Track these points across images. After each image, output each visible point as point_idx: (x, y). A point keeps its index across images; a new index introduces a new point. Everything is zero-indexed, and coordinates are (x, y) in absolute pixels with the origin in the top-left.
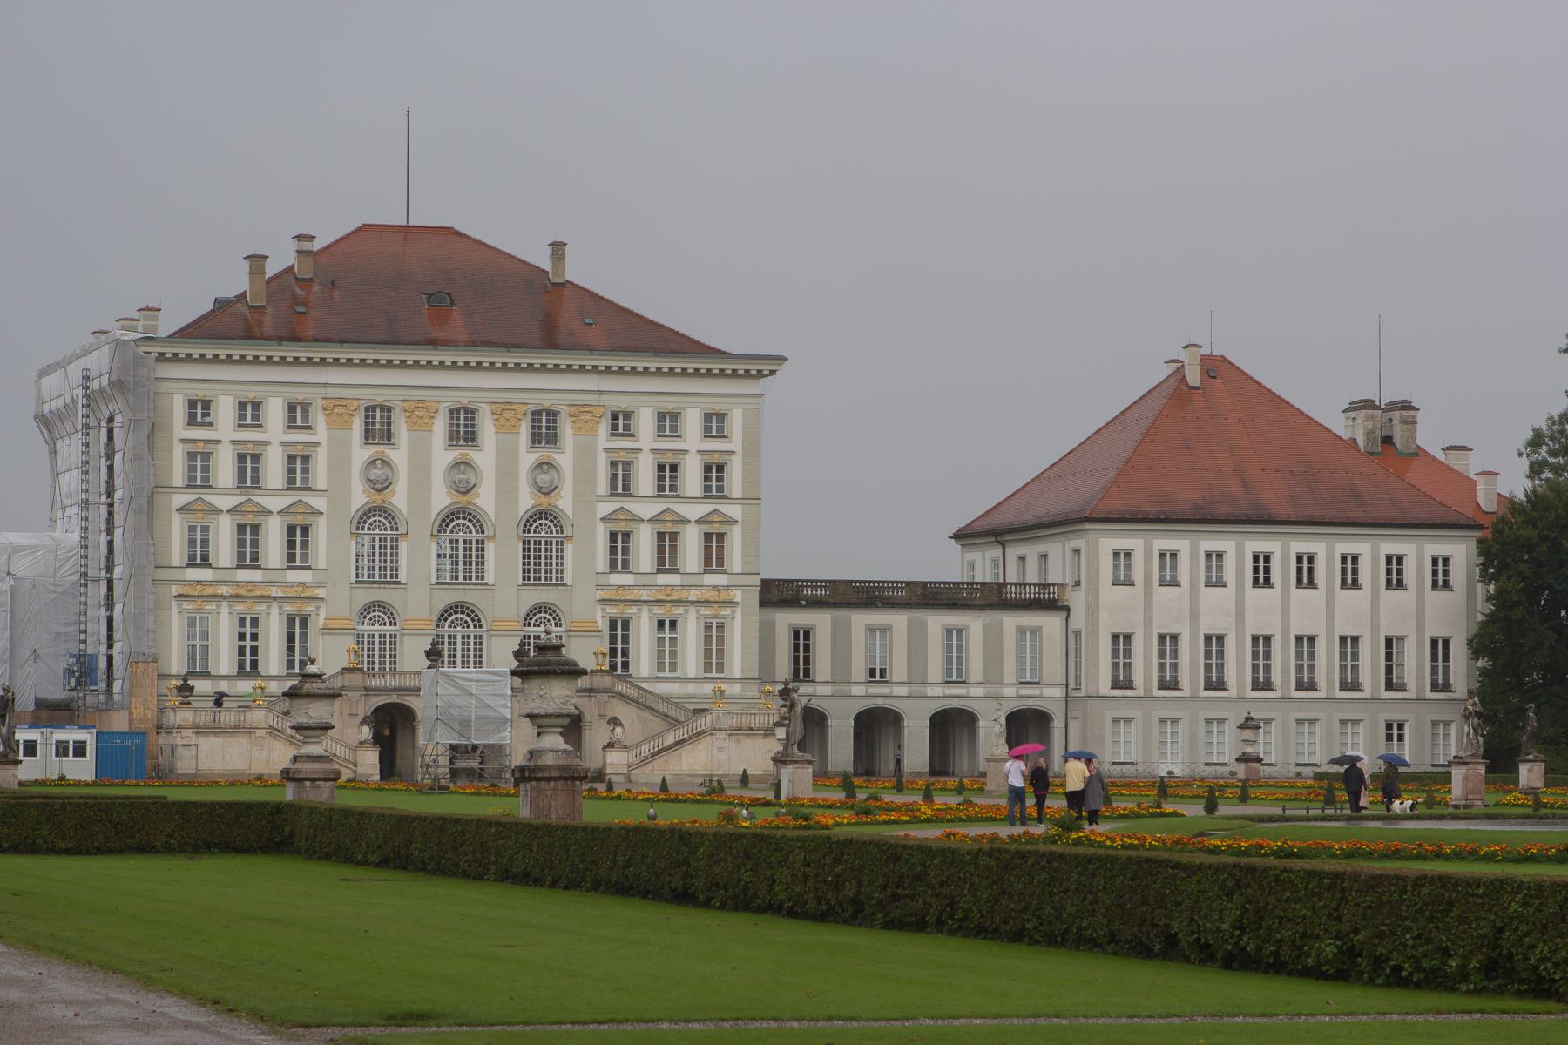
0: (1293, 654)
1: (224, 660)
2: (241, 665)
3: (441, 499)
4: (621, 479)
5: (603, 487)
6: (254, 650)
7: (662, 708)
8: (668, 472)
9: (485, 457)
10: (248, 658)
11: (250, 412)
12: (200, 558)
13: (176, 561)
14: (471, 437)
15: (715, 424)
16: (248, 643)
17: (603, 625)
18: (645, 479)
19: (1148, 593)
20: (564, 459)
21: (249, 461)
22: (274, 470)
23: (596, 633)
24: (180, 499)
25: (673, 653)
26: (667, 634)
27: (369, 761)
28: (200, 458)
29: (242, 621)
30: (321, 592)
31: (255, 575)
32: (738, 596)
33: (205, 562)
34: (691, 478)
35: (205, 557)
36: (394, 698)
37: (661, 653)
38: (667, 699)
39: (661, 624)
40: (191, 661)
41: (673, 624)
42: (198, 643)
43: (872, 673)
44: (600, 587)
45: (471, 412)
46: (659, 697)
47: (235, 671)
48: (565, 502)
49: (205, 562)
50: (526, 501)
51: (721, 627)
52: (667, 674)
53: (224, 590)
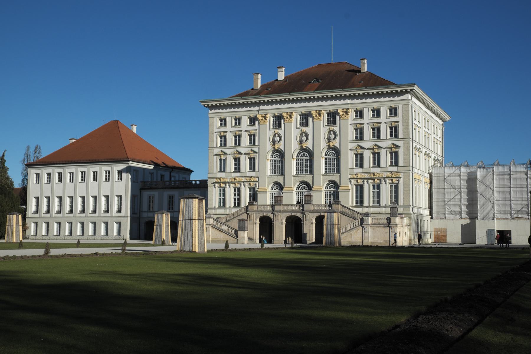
4: (360, 136)
6: (239, 199)
11: (238, 121)
12: (223, 170)
13: (215, 172)
16: (237, 197)
20: (336, 128)
22: (245, 140)
25: (379, 197)
26: (376, 190)
32: (401, 175)
33: (224, 171)
35: (224, 169)
36: (265, 214)
39: (374, 186)
41: (379, 187)
42: (222, 197)
44: (351, 174)
46: (358, 213)
47: (233, 205)
49: (224, 171)
52: (376, 204)
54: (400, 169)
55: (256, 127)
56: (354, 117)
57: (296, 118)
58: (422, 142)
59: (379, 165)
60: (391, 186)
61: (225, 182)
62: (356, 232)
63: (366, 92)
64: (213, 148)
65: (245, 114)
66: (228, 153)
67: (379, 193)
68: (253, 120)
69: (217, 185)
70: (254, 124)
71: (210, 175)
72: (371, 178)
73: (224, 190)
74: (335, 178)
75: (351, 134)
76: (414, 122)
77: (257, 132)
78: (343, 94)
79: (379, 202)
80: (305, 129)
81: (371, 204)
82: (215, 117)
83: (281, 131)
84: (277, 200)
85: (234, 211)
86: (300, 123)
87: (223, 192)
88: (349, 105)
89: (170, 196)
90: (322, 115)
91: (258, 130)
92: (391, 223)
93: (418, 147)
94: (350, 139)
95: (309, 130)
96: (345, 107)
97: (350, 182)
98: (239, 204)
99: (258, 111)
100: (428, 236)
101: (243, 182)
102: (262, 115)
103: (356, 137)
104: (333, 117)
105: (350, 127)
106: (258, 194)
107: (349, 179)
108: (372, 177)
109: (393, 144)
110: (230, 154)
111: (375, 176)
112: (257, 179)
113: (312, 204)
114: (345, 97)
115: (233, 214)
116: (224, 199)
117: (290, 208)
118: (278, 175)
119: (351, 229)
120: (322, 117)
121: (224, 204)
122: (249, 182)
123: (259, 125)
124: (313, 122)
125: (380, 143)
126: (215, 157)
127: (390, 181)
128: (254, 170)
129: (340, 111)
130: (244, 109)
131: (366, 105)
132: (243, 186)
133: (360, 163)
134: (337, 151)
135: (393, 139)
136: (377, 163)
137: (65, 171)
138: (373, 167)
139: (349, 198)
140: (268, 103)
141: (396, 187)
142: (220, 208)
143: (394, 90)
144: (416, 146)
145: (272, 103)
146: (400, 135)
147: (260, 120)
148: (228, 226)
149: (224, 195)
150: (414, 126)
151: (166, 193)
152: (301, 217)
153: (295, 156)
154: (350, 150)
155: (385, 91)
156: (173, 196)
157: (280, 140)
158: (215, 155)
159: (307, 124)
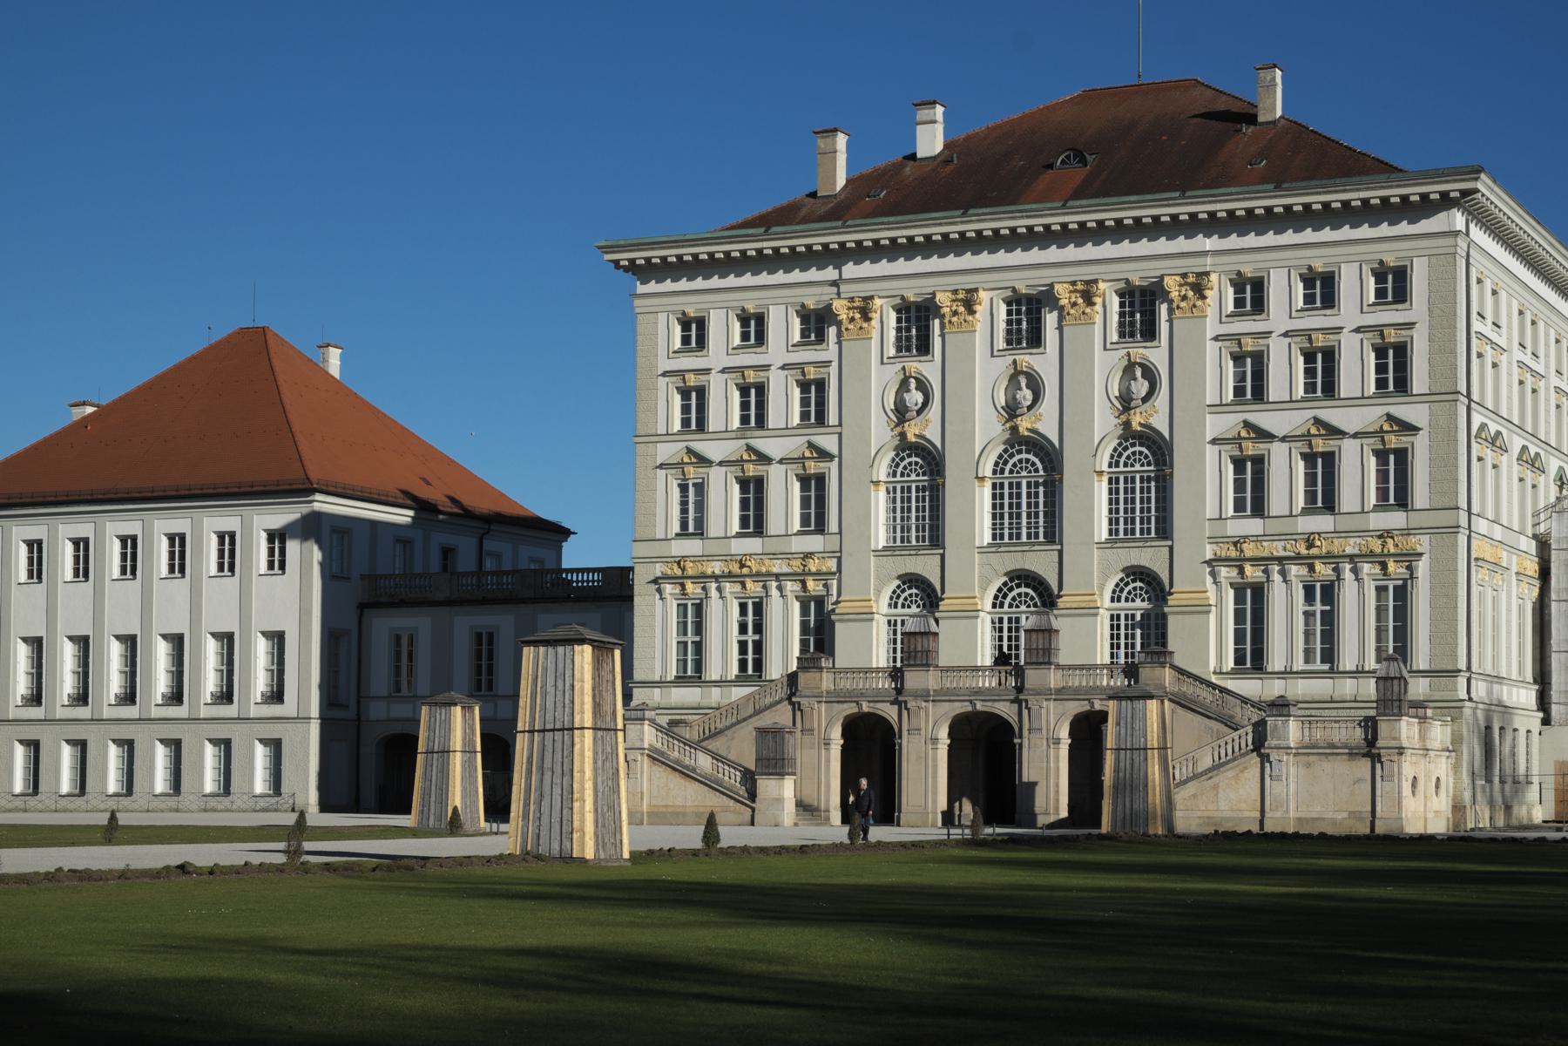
4: (1253, 382)
6: (758, 647)
11: (754, 327)
12: (694, 525)
16: (751, 637)
20: (1156, 355)
22: (785, 403)
24: (668, 451)
25: (1330, 636)
26: (1318, 607)
32: (1422, 543)
33: (700, 532)
35: (700, 522)
36: (866, 708)
40: (683, 663)
42: (691, 638)
44: (1214, 540)
46: (1244, 700)
47: (734, 670)
49: (700, 532)
54: (1417, 520)
55: (829, 351)
56: (1230, 307)
57: (992, 312)
58: (1510, 405)
59: (1330, 506)
60: (1381, 590)
61: (703, 576)
62: (1237, 778)
63: (1278, 203)
64: (655, 438)
65: (782, 297)
66: (716, 458)
67: (1329, 619)
68: (816, 323)
69: (668, 589)
70: (821, 338)
71: (641, 550)
72: (1297, 558)
73: (699, 609)
74: (1152, 557)
75: (1216, 375)
76: (1477, 326)
77: (833, 370)
78: (1183, 211)
79: (1329, 655)
80: (1027, 359)
81: (1299, 664)
82: (658, 313)
83: (929, 369)
84: (915, 649)
85: (739, 693)
86: (1009, 332)
87: (695, 618)
88: (1209, 260)
89: (479, 635)
90: (1098, 300)
91: (835, 365)
92: (1380, 743)
93: (1493, 428)
94: (1211, 397)
95: (1044, 363)
96: (1194, 265)
97: (1213, 574)
98: (758, 665)
99: (834, 283)
100: (1533, 794)
101: (777, 576)
102: (852, 300)
103: (1239, 391)
104: (1142, 308)
105: (1211, 348)
106: (839, 627)
107: (1209, 562)
108: (1304, 552)
109: (1390, 418)
110: (721, 464)
111: (1314, 551)
112: (832, 565)
113: (1058, 667)
114: (1193, 226)
115: (736, 707)
116: (699, 647)
117: (967, 682)
118: (917, 548)
119: (1216, 767)
120: (1099, 308)
121: (699, 666)
123: (839, 343)
124: (1060, 328)
125: (1334, 415)
126: (661, 473)
127: (1377, 570)
128: (821, 528)
129: (1171, 283)
130: (781, 277)
131: (1281, 259)
132: (774, 592)
133: (1253, 499)
134: (1158, 448)
135: (1388, 395)
136: (1324, 496)
137: (53, 534)
138: (1306, 511)
139: (1206, 641)
140: (876, 252)
141: (1402, 593)
142: (681, 680)
143: (1394, 193)
144: (1483, 426)
145: (894, 250)
147: (846, 324)
148: (716, 757)
149: (699, 628)
150: (1474, 341)
151: (465, 624)
152: (1012, 717)
153: (987, 469)
154: (1214, 441)
155: (1355, 197)
156: (491, 636)
157: (925, 404)
158: (661, 466)
159: (1035, 339)
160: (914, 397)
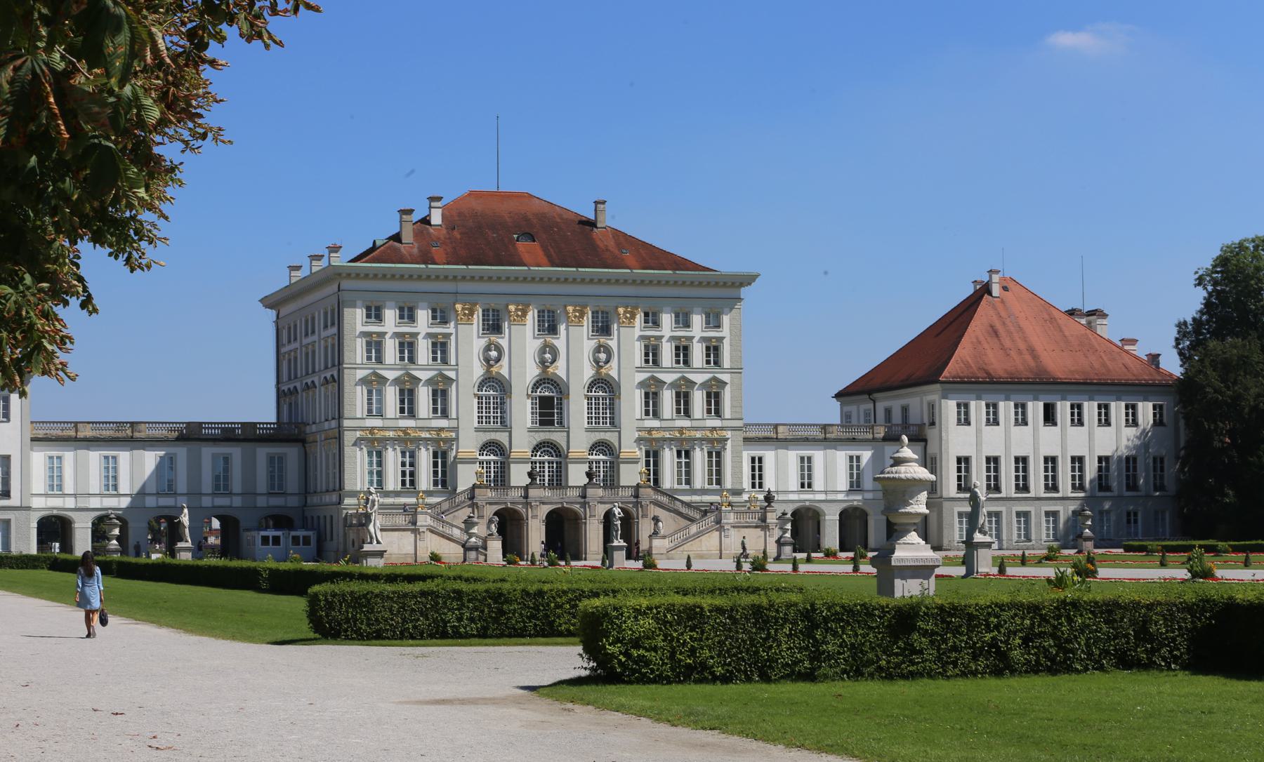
0: (1042, 469)
1: (392, 482)
2: (403, 483)
3: (532, 372)
5: (638, 359)
6: (412, 474)
7: (684, 510)
8: (683, 352)
9: (560, 342)
10: (408, 478)
13: (359, 416)
14: (553, 330)
15: (713, 321)
17: (640, 454)
18: (667, 354)
19: (979, 431)
20: (613, 343)
21: (407, 346)
22: (423, 351)
23: (635, 461)
24: (361, 374)
25: (688, 473)
26: (683, 460)
27: (496, 546)
28: (375, 345)
29: (403, 454)
30: (454, 435)
31: (410, 423)
32: (728, 434)
33: (380, 414)
34: (698, 354)
37: (679, 473)
38: (688, 505)
43: (803, 485)
45: (552, 313)
47: (399, 487)
48: (612, 371)
49: (380, 414)
50: (588, 373)
51: (718, 454)
52: (684, 486)
53: (391, 434)
54: (726, 423)
55: (451, 328)
81: (707, 486)
98: (412, 483)
106: (512, 466)
116: (380, 474)
122: (436, 441)
146: (726, 363)
160: (494, 354)
